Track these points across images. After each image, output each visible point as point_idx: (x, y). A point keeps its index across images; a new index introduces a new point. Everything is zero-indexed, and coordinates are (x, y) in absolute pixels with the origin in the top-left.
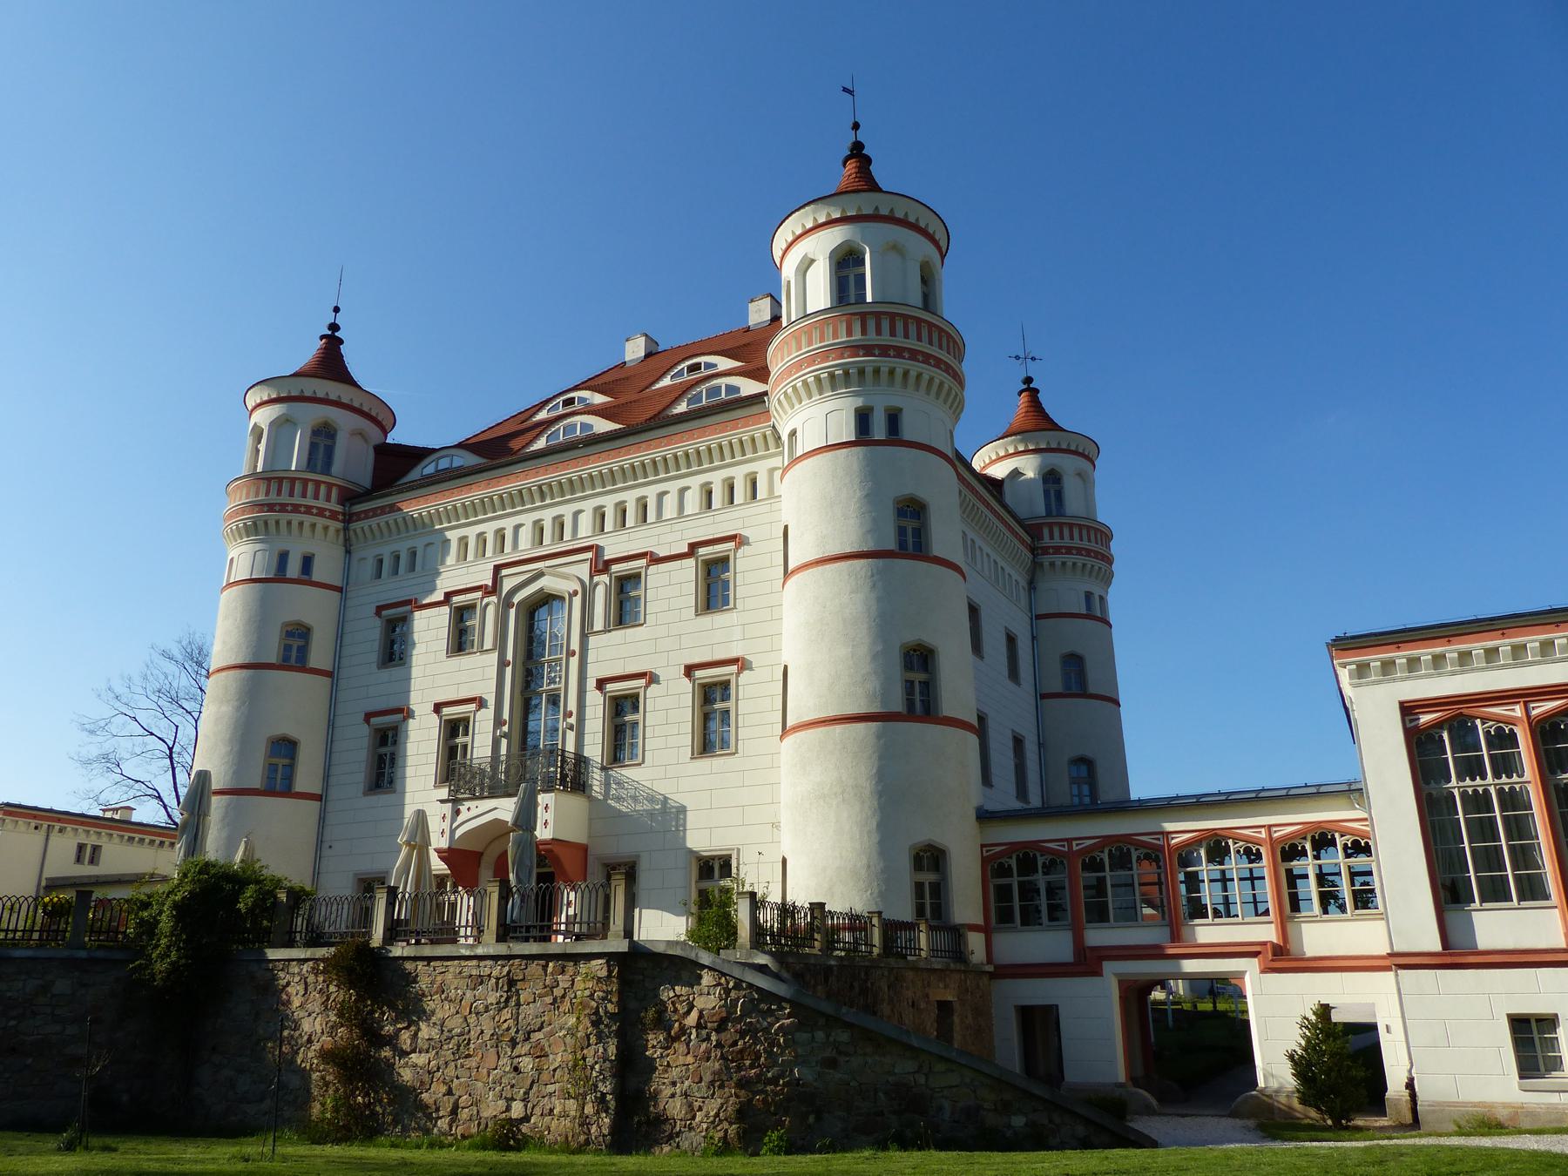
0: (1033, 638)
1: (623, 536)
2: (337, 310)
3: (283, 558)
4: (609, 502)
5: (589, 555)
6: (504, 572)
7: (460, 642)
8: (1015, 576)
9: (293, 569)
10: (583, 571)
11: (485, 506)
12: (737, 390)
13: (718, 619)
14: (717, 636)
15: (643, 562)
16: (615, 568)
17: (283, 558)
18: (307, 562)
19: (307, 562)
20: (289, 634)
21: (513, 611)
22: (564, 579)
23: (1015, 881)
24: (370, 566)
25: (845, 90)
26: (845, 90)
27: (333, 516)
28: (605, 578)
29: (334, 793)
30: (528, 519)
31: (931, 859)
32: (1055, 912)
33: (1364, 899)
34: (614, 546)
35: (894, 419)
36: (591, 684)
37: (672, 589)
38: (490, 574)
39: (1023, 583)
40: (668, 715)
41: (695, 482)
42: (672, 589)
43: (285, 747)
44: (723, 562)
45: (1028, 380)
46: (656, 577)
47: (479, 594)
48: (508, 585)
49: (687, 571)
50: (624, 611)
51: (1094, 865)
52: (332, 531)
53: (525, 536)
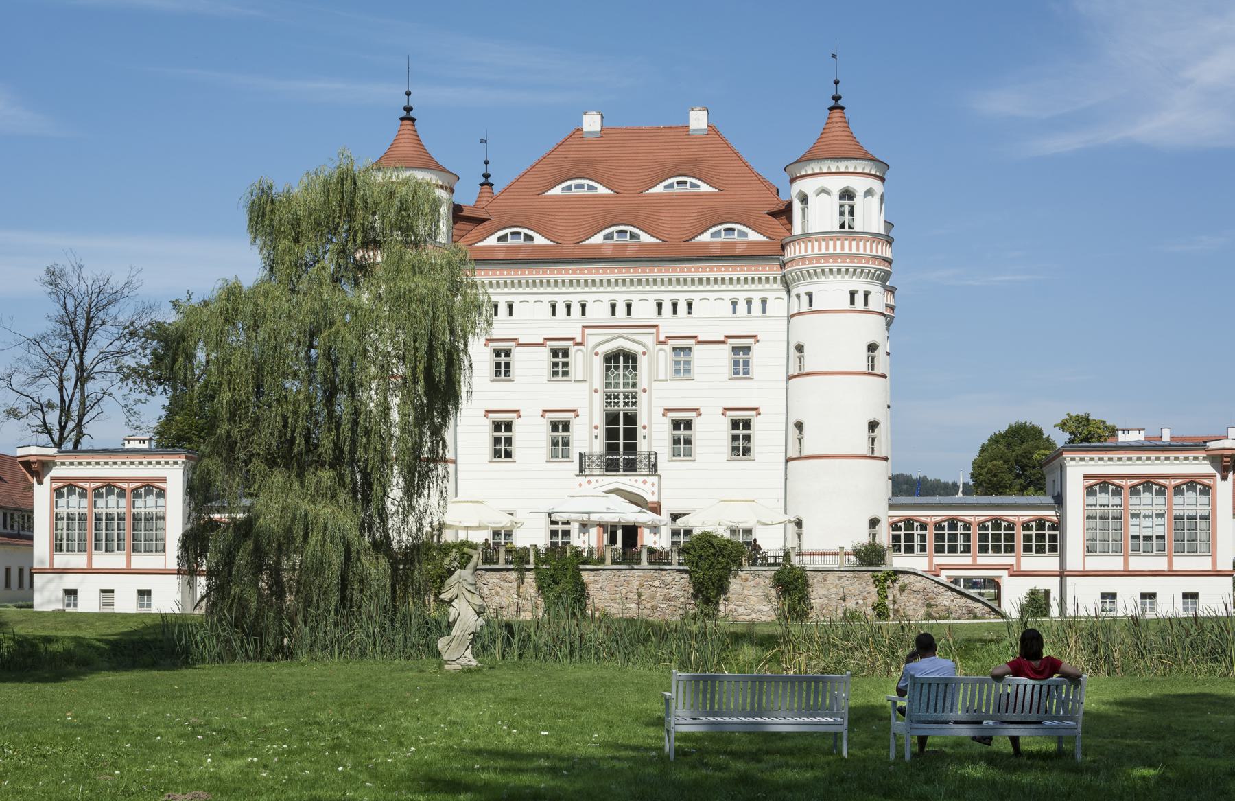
5: (653, 330)
6: (587, 331)
10: (649, 340)
12: (745, 235)
14: (741, 394)
15: (693, 341)
16: (670, 342)
23: (902, 533)
29: (459, 462)
31: (874, 523)
33: (1053, 549)
34: (670, 326)
35: (866, 294)
38: (580, 330)
40: (712, 434)
44: (747, 349)
47: (571, 343)
48: (592, 341)
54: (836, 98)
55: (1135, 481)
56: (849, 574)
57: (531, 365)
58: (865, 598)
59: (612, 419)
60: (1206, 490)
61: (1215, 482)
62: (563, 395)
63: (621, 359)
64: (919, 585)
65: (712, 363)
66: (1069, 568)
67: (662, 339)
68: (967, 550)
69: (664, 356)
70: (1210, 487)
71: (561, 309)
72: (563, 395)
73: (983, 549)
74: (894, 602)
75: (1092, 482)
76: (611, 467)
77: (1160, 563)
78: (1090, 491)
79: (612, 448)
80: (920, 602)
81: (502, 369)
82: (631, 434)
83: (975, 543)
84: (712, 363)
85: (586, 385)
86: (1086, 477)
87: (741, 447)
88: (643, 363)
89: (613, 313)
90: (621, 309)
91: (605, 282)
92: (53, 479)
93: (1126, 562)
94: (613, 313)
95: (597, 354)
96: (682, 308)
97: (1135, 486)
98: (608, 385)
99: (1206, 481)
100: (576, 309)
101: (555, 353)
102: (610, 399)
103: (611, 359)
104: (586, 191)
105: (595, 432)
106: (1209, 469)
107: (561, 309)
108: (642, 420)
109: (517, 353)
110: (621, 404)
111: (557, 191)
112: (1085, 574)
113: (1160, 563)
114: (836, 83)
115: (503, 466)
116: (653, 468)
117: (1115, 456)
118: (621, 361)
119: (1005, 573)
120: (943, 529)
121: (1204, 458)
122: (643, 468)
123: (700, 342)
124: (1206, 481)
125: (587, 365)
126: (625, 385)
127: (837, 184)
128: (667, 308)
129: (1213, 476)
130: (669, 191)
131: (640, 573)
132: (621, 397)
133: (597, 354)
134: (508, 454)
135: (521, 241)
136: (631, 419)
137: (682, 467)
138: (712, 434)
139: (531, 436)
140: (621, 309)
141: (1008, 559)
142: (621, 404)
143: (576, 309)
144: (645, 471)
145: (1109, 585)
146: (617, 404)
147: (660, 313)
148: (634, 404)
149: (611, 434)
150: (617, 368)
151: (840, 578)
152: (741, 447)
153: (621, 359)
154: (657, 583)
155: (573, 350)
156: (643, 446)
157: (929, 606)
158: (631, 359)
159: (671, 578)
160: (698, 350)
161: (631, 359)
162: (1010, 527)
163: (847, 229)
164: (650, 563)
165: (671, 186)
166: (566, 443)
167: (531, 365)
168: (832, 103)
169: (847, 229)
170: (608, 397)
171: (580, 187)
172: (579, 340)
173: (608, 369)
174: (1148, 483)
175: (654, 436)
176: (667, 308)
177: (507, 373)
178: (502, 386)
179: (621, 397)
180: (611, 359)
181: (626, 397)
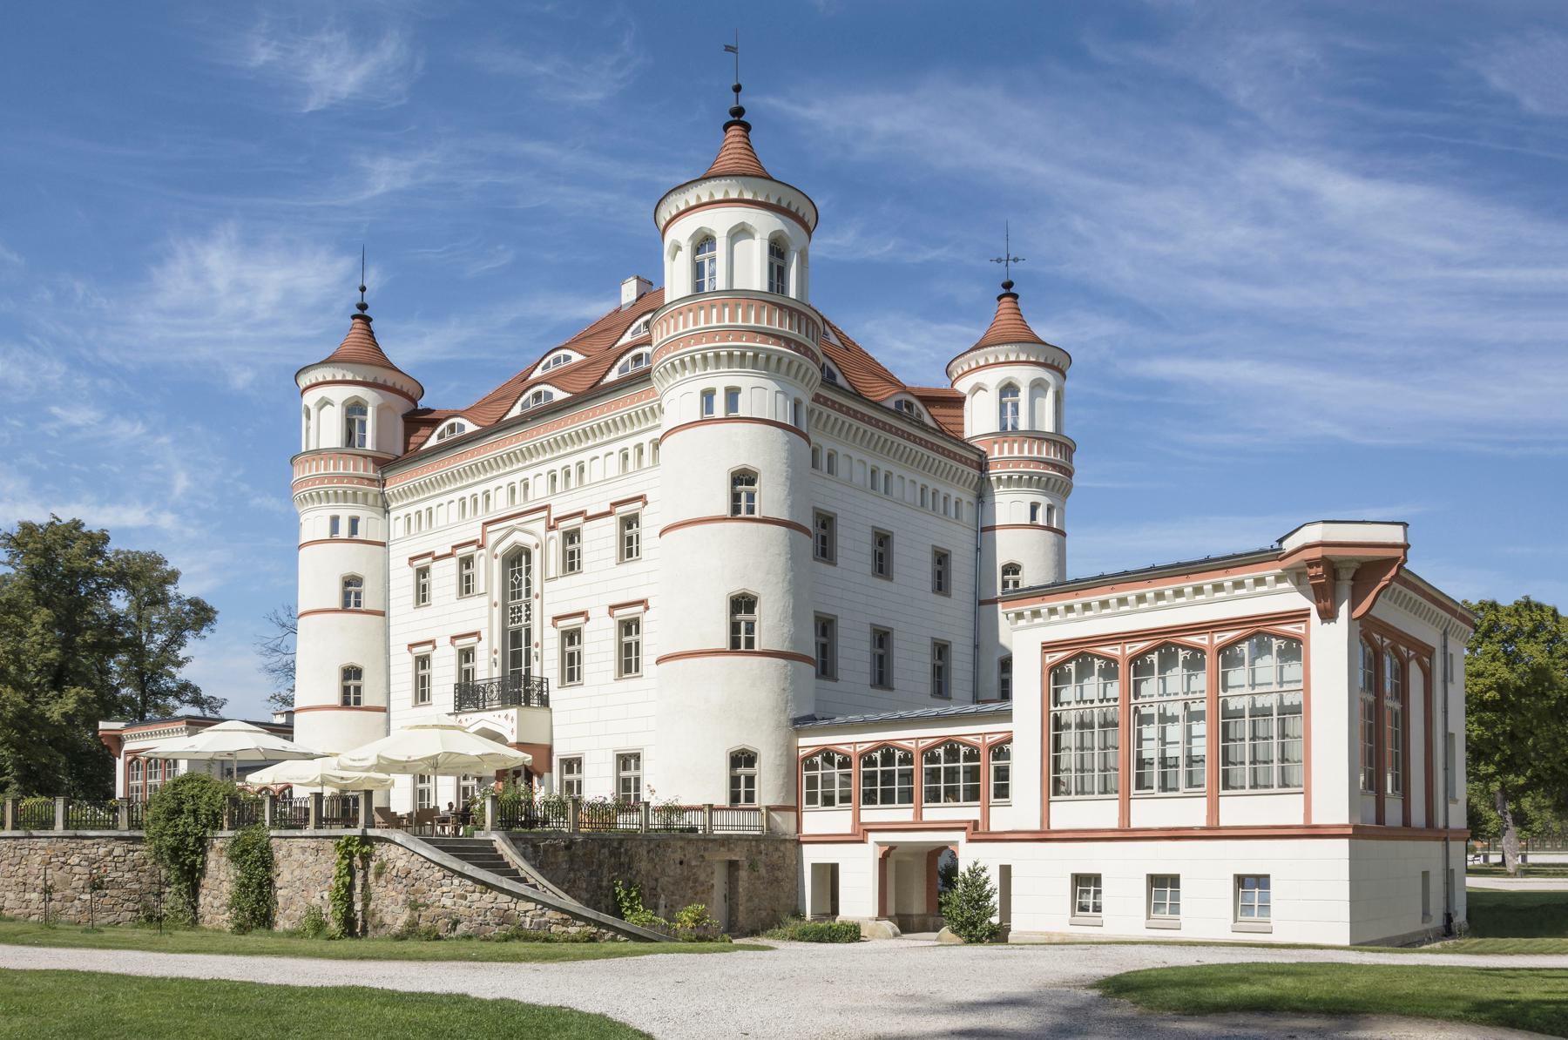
0: (978, 549)
3: (335, 521)
4: (558, 466)
5: (545, 513)
6: (489, 528)
7: (466, 586)
8: (954, 494)
9: (344, 531)
10: (540, 527)
11: (473, 470)
13: (631, 567)
14: (629, 581)
15: (580, 519)
16: (562, 525)
18: (354, 522)
19: (354, 522)
21: (497, 565)
22: (532, 534)
24: (401, 523)
27: (371, 480)
30: (504, 481)
31: (742, 759)
32: (846, 799)
36: (548, 621)
37: (600, 540)
38: (479, 530)
39: (967, 497)
40: (600, 644)
42: (600, 540)
46: (589, 531)
47: (474, 547)
48: (492, 539)
49: (611, 526)
50: (571, 563)
51: (871, 762)
52: (371, 498)
53: (503, 494)
55: (1140, 646)
56: (313, 843)
57: (444, 576)
60: (1294, 649)
61: (1308, 629)
64: (400, 864)
66: (1037, 827)
68: (907, 797)
70: (1299, 642)
73: (933, 796)
74: (367, 899)
75: (1060, 656)
77: (1191, 812)
78: (1056, 675)
80: (402, 897)
81: (422, 595)
83: (919, 785)
85: (485, 599)
86: (1048, 647)
87: (628, 661)
92: (127, 753)
93: (1125, 812)
97: (1141, 655)
99: (1289, 629)
104: (563, 365)
106: (1296, 600)
108: (535, 638)
112: (1044, 836)
113: (1191, 812)
116: (544, 701)
117: (1094, 598)
119: (960, 837)
120: (874, 764)
121: (1279, 579)
122: (535, 702)
124: (1289, 629)
125: (489, 573)
129: (1303, 615)
131: (43, 843)
137: (572, 692)
141: (971, 812)
144: (535, 702)
145: (1087, 858)
150: (520, 572)
151: (304, 850)
152: (628, 661)
154: (74, 860)
156: (535, 672)
157: (414, 906)
158: (528, 554)
159: (102, 851)
162: (973, 755)
164: (66, 827)
167: (444, 576)
174: (1166, 648)
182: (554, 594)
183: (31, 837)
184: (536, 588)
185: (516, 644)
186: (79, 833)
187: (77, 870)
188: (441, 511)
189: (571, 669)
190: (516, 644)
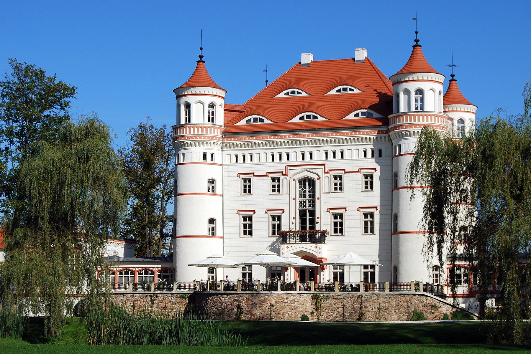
1: (335, 162)
2: (201, 49)
3: (205, 155)
5: (323, 167)
6: (289, 168)
10: (320, 172)
16: (331, 172)
17: (205, 155)
20: (209, 182)
25: (414, 19)
26: (414, 19)
28: (328, 175)
34: (331, 164)
40: (353, 222)
41: (361, 148)
43: (212, 221)
45: (452, 76)
47: (281, 174)
48: (291, 173)
54: (417, 41)
56: (391, 296)
57: (261, 185)
58: (399, 309)
59: (303, 214)
62: (279, 202)
63: (307, 183)
64: (428, 302)
65: (353, 183)
67: (326, 171)
69: (328, 182)
71: (277, 157)
72: (279, 202)
76: (303, 239)
79: (303, 228)
81: (248, 189)
82: (312, 222)
84: (353, 183)
87: (369, 228)
88: (317, 183)
89: (303, 158)
90: (307, 156)
91: (298, 143)
94: (303, 158)
95: (294, 180)
96: (338, 155)
98: (301, 196)
100: (284, 157)
101: (274, 180)
102: (302, 203)
103: (302, 181)
104: (296, 95)
105: (294, 221)
107: (277, 157)
108: (317, 214)
109: (254, 180)
110: (307, 206)
111: (281, 95)
114: (417, 33)
115: (247, 239)
118: (308, 184)
123: (345, 172)
126: (310, 196)
127: (412, 87)
128: (331, 155)
130: (339, 93)
132: (307, 202)
133: (294, 180)
134: (250, 233)
135: (258, 122)
136: (312, 213)
137: (338, 238)
138: (353, 222)
139: (262, 225)
140: (307, 156)
142: (307, 206)
143: (284, 157)
146: (305, 206)
147: (327, 157)
148: (313, 206)
149: (303, 222)
150: (305, 187)
153: (307, 183)
155: (282, 178)
156: (317, 227)
158: (312, 182)
159: (294, 298)
160: (345, 177)
161: (312, 182)
163: (419, 110)
165: (339, 90)
166: (279, 226)
167: (261, 185)
168: (415, 43)
169: (419, 110)
170: (301, 202)
171: (293, 93)
172: (284, 173)
173: (301, 187)
175: (324, 222)
176: (331, 155)
177: (250, 191)
178: (248, 197)
179: (307, 202)
180: (302, 181)
181: (310, 202)
182: (326, 201)
183: (272, 293)
184: (317, 195)
185: (308, 217)
186: (288, 292)
187: (287, 304)
188: (263, 158)
189: (339, 228)
190: (308, 217)
